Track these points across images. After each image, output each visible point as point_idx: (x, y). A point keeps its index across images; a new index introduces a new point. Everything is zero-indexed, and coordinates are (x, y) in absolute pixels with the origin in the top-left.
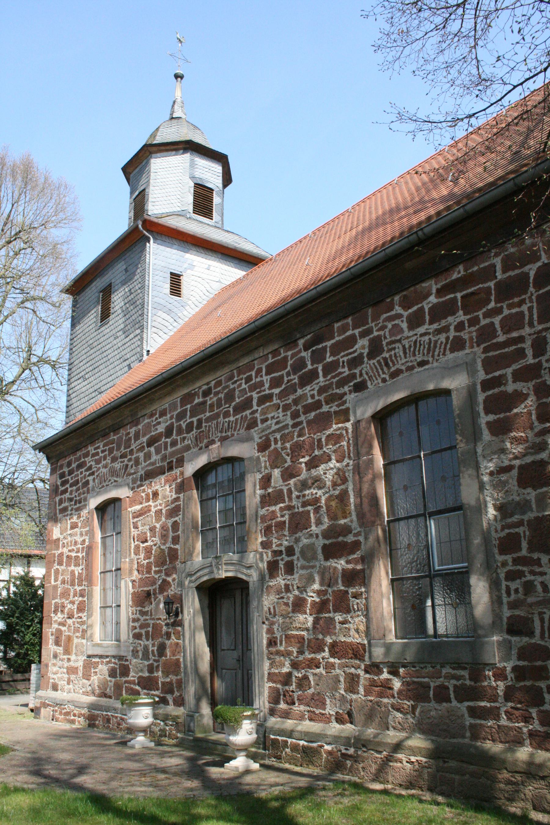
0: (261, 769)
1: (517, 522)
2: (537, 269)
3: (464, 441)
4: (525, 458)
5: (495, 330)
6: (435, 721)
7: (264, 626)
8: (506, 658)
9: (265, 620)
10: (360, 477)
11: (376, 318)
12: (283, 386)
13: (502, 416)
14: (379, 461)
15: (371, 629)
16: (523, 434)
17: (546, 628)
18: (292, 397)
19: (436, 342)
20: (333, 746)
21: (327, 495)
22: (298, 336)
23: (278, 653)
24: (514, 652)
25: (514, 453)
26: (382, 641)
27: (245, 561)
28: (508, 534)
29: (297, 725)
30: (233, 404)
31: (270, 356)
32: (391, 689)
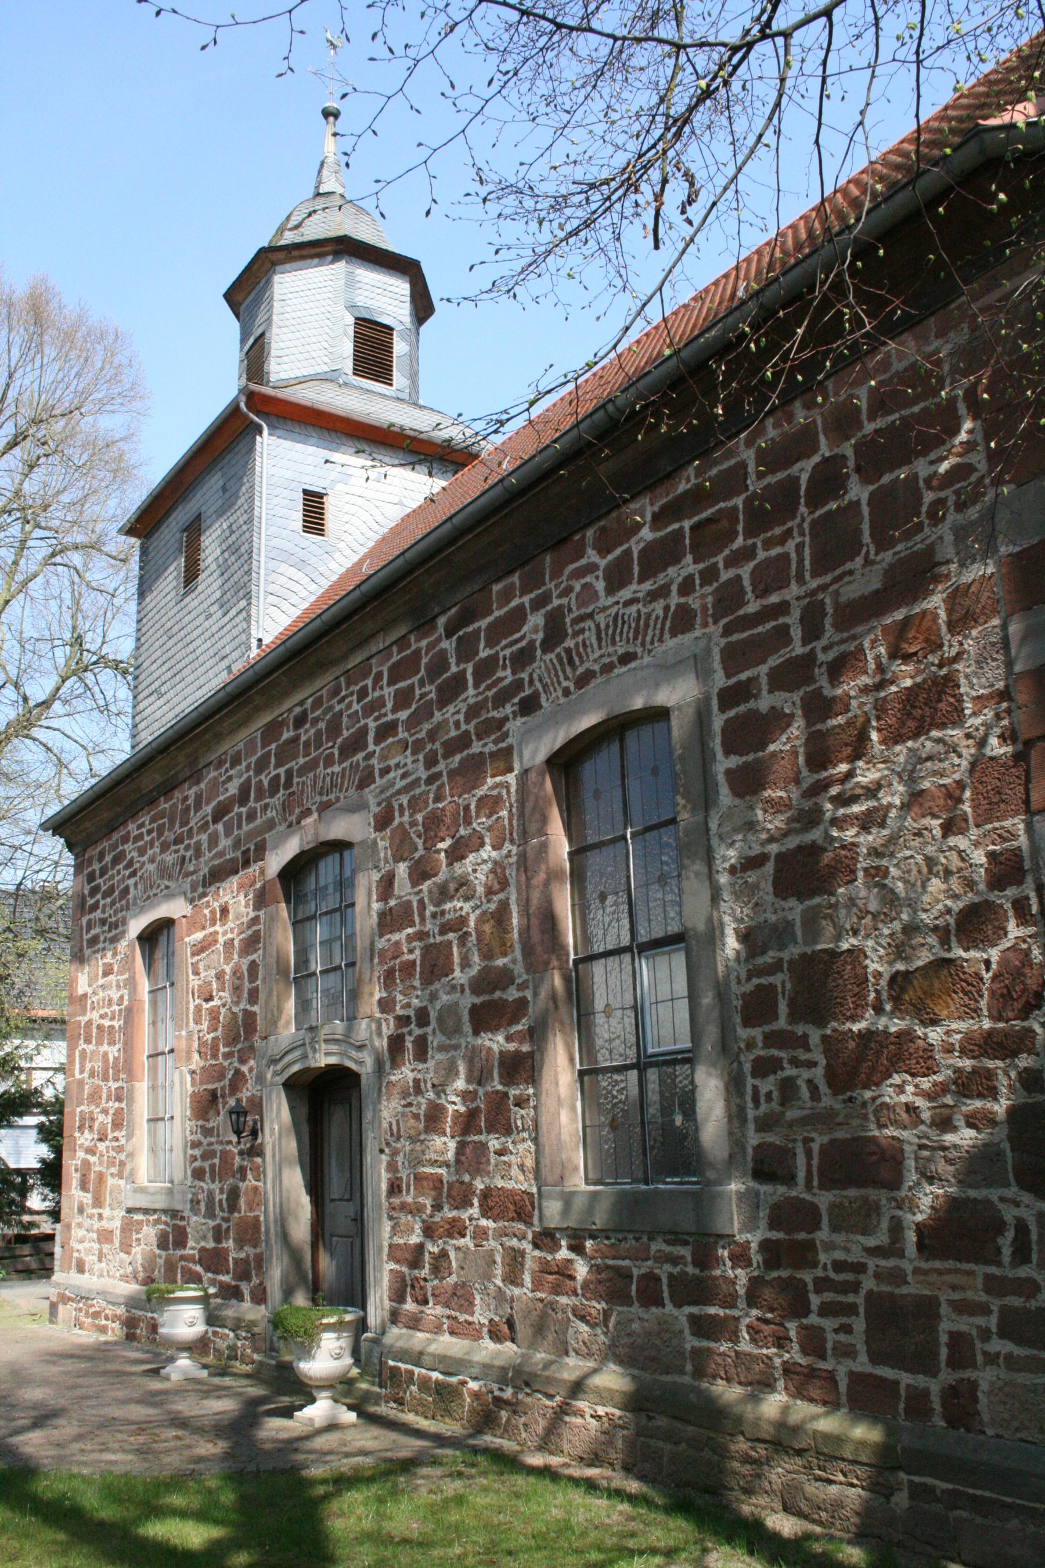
0: (361, 1421)
1: (770, 965)
2: (814, 468)
3: (689, 806)
4: (786, 840)
5: (742, 591)
6: (639, 1340)
7: (384, 1157)
8: (750, 1225)
9: (384, 1146)
10: (528, 879)
11: (556, 574)
12: (414, 706)
13: (750, 757)
14: (561, 846)
15: (542, 1165)
16: (782, 794)
17: (815, 1169)
18: (427, 726)
19: (648, 616)
20: (481, 1382)
21: (478, 912)
22: (436, 610)
23: (403, 1207)
24: (764, 1214)
25: (769, 830)
26: (558, 1188)
27: (353, 1035)
28: (759, 987)
29: (430, 1342)
30: (339, 740)
31: (395, 649)
32: (572, 1278)
